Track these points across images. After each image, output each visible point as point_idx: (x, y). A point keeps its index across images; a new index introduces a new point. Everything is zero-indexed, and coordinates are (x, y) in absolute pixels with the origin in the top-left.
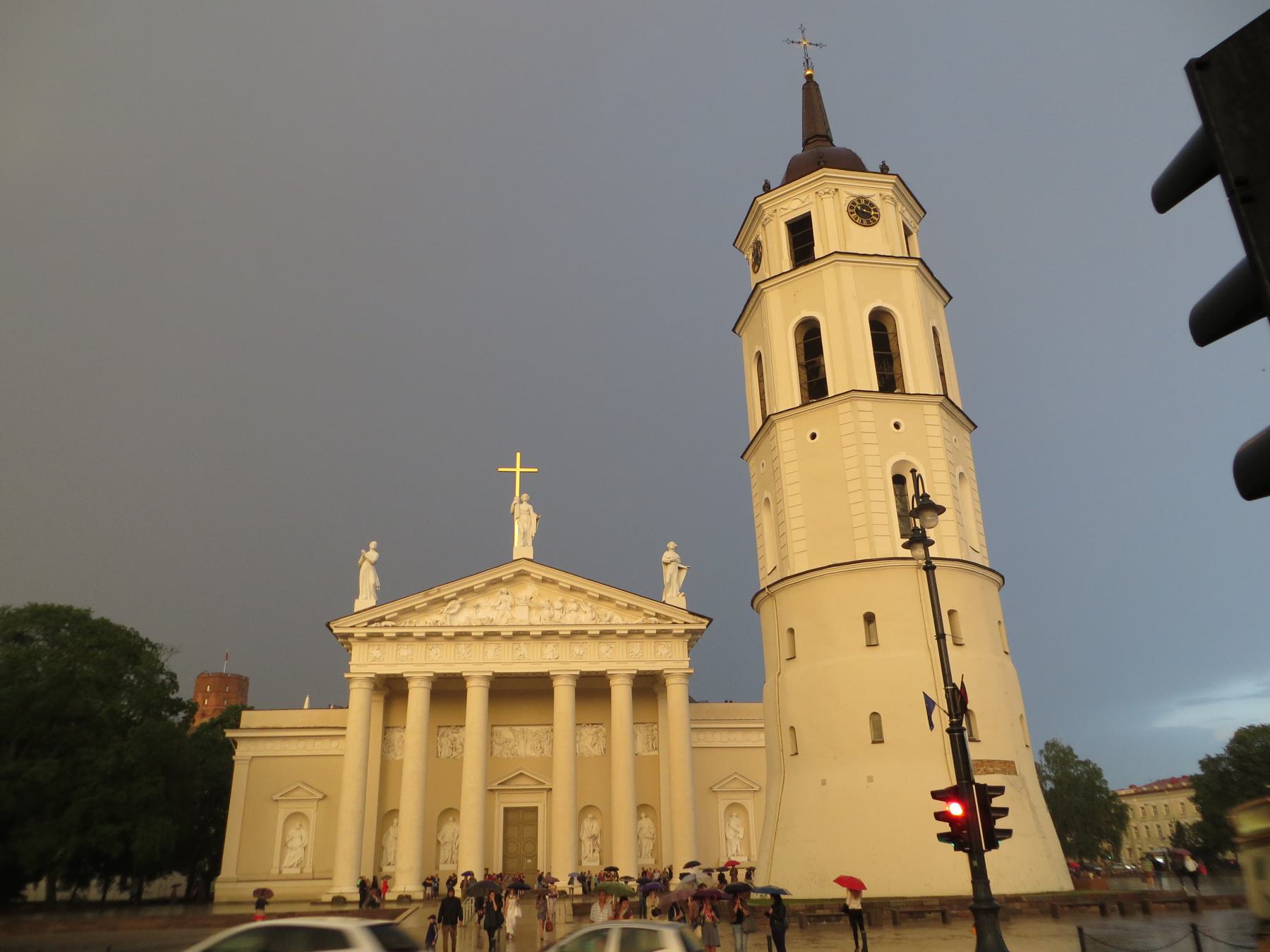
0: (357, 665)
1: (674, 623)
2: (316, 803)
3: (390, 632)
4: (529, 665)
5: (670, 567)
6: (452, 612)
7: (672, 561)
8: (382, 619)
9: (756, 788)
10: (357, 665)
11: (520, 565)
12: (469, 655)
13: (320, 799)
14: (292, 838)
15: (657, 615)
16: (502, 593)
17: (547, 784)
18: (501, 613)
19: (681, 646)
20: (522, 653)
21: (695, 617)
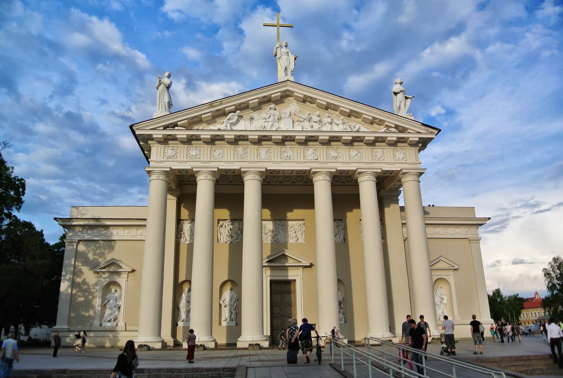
0: (156, 162)
1: (409, 132)
2: (126, 275)
3: (182, 134)
4: (294, 164)
5: (398, 95)
6: (231, 122)
7: (401, 91)
8: (174, 125)
9: (456, 267)
10: (156, 162)
11: (286, 86)
12: (246, 155)
13: (130, 272)
14: (109, 301)
15: (396, 127)
16: (271, 108)
17: (303, 262)
18: (270, 123)
19: (413, 152)
20: (289, 155)
21: (427, 128)
